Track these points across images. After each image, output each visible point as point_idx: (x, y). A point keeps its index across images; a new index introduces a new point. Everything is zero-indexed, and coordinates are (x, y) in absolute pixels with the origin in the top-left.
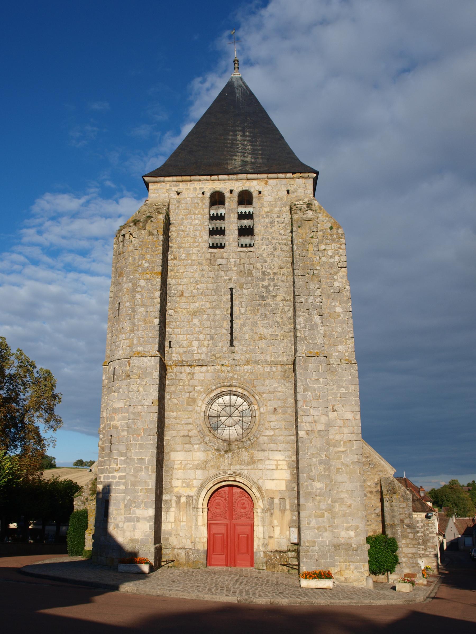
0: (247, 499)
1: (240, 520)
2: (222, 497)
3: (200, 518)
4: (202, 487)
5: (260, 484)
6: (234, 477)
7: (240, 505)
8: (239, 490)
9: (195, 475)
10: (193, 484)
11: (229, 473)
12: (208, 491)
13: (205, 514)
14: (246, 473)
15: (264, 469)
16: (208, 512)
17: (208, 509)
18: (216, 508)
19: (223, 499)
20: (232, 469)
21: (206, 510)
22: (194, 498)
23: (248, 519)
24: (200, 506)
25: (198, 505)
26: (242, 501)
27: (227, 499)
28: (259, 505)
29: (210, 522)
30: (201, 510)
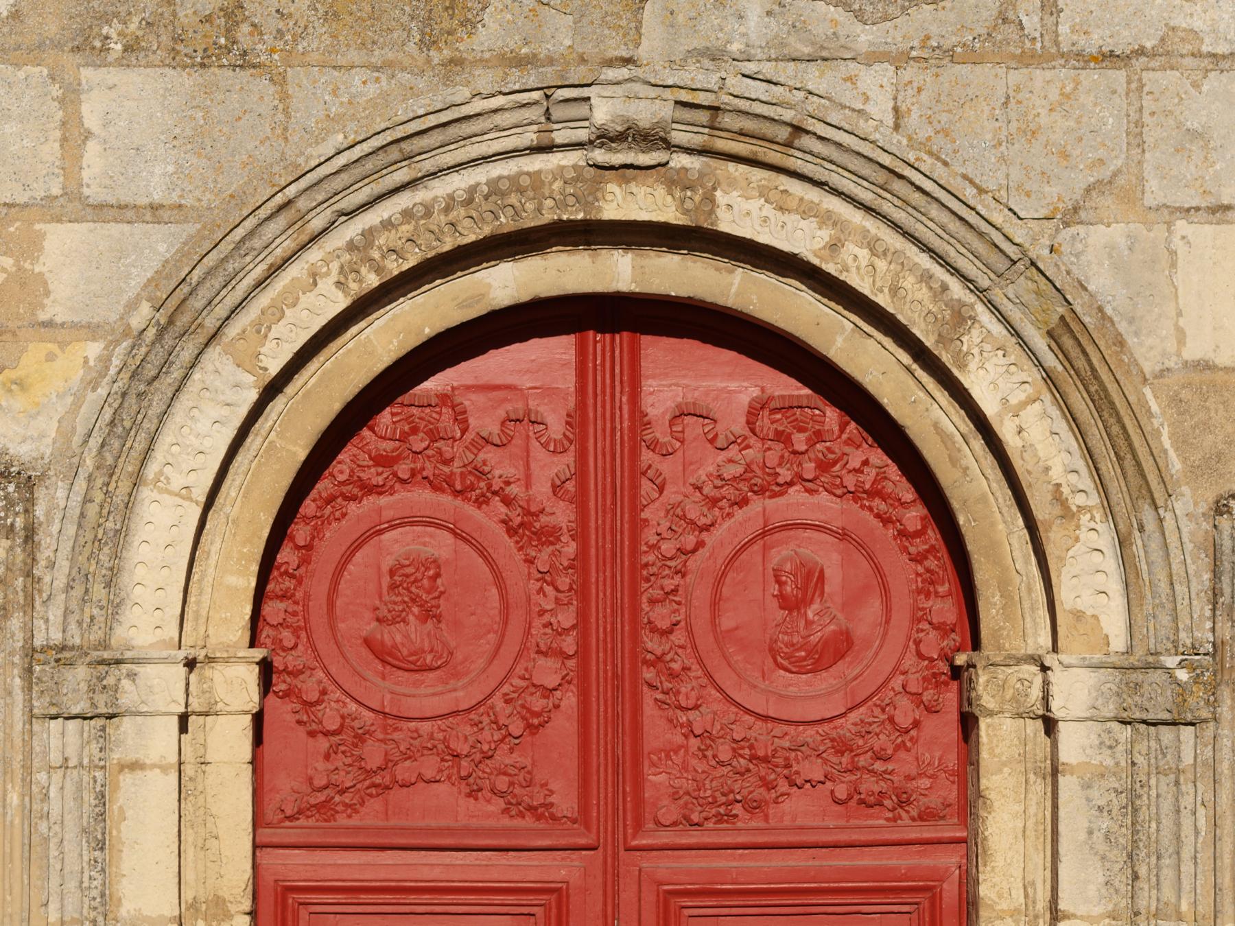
0: (862, 519)
1: (747, 827)
2: (474, 487)
3: (146, 806)
4: (178, 329)
5: (1101, 282)
6: (678, 182)
7: (751, 607)
8: (738, 384)
9: (73, 137)
10: (31, 286)
11: (605, 110)
12: (272, 390)
13: (229, 740)
14: (880, 108)
15: (1162, 53)
16: (258, 720)
17: (266, 670)
18: (381, 653)
19: (487, 521)
20: (651, 46)
21: (237, 685)
22: (57, 502)
23: (876, 824)
24: (146, 620)
25: (114, 608)
26: (783, 553)
27: (561, 515)
28: (1076, 609)
29: (297, 866)
30: (163, 686)
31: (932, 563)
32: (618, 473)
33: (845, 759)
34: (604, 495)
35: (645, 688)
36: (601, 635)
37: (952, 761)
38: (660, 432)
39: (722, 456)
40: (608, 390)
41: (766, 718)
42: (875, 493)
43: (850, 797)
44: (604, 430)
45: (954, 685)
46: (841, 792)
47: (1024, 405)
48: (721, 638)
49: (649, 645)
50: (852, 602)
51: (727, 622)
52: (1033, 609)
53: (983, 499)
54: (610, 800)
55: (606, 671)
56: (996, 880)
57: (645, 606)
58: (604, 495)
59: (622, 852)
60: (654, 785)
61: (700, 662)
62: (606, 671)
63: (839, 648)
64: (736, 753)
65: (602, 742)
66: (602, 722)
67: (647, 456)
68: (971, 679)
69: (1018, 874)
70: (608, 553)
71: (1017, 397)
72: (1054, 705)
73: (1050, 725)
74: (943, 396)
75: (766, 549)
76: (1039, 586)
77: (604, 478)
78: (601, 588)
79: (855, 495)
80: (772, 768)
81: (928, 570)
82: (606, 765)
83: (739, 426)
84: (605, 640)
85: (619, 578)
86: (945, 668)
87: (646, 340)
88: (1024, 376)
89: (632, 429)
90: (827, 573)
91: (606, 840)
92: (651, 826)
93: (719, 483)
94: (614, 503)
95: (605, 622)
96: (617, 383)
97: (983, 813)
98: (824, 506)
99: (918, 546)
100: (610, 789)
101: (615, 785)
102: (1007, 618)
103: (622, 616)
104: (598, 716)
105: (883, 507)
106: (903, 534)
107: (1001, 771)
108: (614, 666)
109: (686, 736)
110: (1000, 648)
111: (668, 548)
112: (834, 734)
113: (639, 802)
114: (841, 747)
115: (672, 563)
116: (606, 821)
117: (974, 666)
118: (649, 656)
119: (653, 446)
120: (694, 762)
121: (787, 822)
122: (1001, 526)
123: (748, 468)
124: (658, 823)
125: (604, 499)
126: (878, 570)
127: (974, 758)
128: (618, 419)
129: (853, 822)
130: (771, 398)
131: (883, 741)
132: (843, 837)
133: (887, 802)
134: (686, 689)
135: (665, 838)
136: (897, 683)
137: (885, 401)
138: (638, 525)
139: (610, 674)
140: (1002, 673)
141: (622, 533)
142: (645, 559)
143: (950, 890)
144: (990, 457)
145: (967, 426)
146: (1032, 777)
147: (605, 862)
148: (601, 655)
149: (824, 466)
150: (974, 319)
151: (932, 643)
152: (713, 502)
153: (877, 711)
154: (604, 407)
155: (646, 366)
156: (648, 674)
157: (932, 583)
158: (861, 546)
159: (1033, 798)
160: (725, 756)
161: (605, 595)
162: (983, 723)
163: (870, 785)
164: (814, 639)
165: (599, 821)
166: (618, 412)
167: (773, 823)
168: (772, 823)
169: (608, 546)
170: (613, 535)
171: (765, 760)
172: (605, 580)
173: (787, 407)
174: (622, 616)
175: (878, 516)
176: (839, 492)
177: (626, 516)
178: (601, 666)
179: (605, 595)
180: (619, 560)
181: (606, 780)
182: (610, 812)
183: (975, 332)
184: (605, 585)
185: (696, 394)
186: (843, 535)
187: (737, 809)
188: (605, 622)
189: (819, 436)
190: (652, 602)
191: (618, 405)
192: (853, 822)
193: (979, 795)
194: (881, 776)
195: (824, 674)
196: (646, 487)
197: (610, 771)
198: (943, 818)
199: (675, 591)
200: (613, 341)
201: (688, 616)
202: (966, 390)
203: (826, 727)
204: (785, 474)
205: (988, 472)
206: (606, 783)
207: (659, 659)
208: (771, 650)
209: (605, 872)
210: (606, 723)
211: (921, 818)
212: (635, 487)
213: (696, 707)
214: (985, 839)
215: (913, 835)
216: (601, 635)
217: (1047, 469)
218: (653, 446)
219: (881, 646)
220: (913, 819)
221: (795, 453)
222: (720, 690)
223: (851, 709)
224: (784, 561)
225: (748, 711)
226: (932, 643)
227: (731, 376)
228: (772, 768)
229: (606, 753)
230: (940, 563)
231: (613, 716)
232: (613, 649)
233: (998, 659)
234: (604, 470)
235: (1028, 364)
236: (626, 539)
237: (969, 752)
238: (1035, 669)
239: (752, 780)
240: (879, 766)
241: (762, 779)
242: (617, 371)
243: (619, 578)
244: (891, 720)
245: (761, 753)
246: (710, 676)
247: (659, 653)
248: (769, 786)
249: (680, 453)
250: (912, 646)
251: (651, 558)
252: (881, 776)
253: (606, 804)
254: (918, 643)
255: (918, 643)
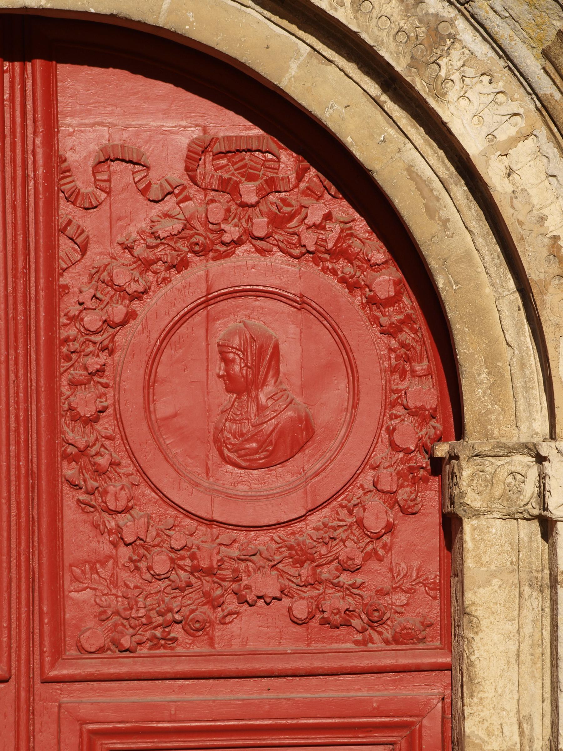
0: (322, 284)
1: (189, 653)
7: (192, 390)
8: (172, 123)
23: (342, 648)
26: (229, 324)
31: (407, 336)
32: (32, 230)
33: (305, 571)
34: (15, 256)
35: (66, 488)
36: (13, 425)
37: (433, 571)
38: (83, 182)
39: (156, 210)
40: (18, 130)
41: (210, 522)
42: (339, 253)
43: (311, 616)
44: (14, 179)
45: (435, 482)
46: (301, 610)
47: (514, 141)
48: (156, 427)
49: (70, 436)
50: (313, 383)
51: (163, 408)
52: (527, 388)
53: (467, 257)
54: (23, 622)
55: (18, 468)
56: (485, 713)
57: (65, 390)
58: (15, 256)
59: (38, 685)
60: (76, 603)
61: (132, 455)
62: (18, 468)
63: (298, 437)
64: (174, 565)
65: (14, 552)
66: (14, 528)
67: (66, 210)
68: (453, 473)
69: (511, 706)
70: (20, 327)
71: (507, 131)
72: (552, 502)
73: (547, 527)
74: (417, 134)
75: (209, 320)
76: (533, 361)
77: (15, 236)
78: (12, 368)
79: (315, 256)
80: (217, 583)
81: (403, 345)
82: (19, 580)
83: (177, 174)
84: (17, 431)
85: (33, 356)
86: (424, 462)
87: (63, 69)
88: (514, 107)
89: (48, 177)
90: (283, 348)
91: (19, 671)
92: (73, 652)
93: (152, 242)
94: (27, 266)
95: (18, 409)
96: (30, 122)
97: (468, 634)
98: (278, 269)
99: (391, 316)
100: (24, 609)
101: (30, 603)
102: (496, 399)
103: (38, 401)
104: (9, 522)
105: (349, 269)
106: (373, 301)
107: (488, 583)
108: (28, 461)
109: (115, 545)
110: (487, 436)
111: (92, 320)
112: (292, 541)
113: (58, 624)
114: (301, 556)
115: (97, 338)
116: (19, 647)
117: (457, 458)
118: (70, 449)
119: (73, 197)
120: (124, 575)
121: (236, 646)
122: (488, 290)
123: (188, 224)
124: (81, 649)
125: (15, 262)
126: (343, 344)
127: (458, 568)
128: (30, 166)
129: (315, 646)
130: (215, 140)
131: (350, 549)
132: (303, 664)
133: (356, 622)
134: (116, 491)
135: (90, 667)
137: (348, 140)
138: (55, 292)
139: (23, 471)
140: (490, 465)
141: (37, 302)
142: (64, 333)
143: (431, 727)
144: (475, 207)
145: (447, 170)
146: (527, 590)
147: (18, 697)
148: (12, 448)
149: (278, 221)
150: (454, 38)
151: (408, 433)
152: (146, 265)
153: (343, 513)
154: (13, 151)
155: (64, 101)
156: (70, 471)
157: (408, 360)
158: (322, 316)
159: (529, 615)
160: (161, 568)
161: (17, 376)
162: (468, 526)
163: (335, 601)
164: (267, 427)
165: (10, 648)
166: (30, 156)
167: (219, 647)
168: (219, 647)
169: (20, 318)
170: (26, 305)
171: (210, 572)
172: (16, 359)
173: (234, 151)
174: (38, 401)
175: (343, 280)
176: (296, 252)
177: (42, 281)
178: (13, 462)
179: (17, 376)
180: (33, 335)
181: (19, 598)
182: (23, 636)
183: (455, 54)
184: (16, 364)
185: (125, 135)
186: (301, 304)
187: (177, 632)
188: (18, 409)
189: (272, 186)
190: (74, 384)
191: (30, 148)
192: (315, 646)
193: (465, 613)
194: (348, 590)
195: (280, 469)
196: (65, 246)
197: (23, 587)
198: (423, 640)
199: (101, 371)
200: (23, 70)
201: (117, 402)
202: (444, 124)
203: (282, 532)
204: (232, 232)
205: (473, 224)
206: (19, 603)
207: (82, 452)
208: (216, 440)
209: (18, 709)
210: (19, 530)
211: (396, 640)
212: (52, 247)
213: (127, 510)
214: (471, 664)
215: (387, 661)
216: (13, 425)
217: (542, 219)
218: (73, 197)
219: (347, 435)
220: (387, 642)
221: (243, 205)
222: (156, 489)
223: (312, 511)
224: (232, 334)
225: (189, 514)
226: (408, 433)
227: (166, 113)
228: (217, 583)
229: (19, 566)
230: (417, 336)
231: (27, 521)
232: (27, 440)
233: (485, 449)
234: (15, 226)
235: (519, 92)
236: (42, 309)
237: (452, 561)
238: (529, 460)
239: (193, 598)
240: (345, 579)
241: (206, 595)
242: (29, 107)
243: (33, 356)
244: (360, 523)
245: (204, 564)
246: (142, 472)
247: (82, 444)
248: (215, 603)
249: (105, 207)
250: (385, 435)
251: (72, 332)
252: (348, 590)
253: (19, 626)
254: (391, 432)
255: (391, 432)
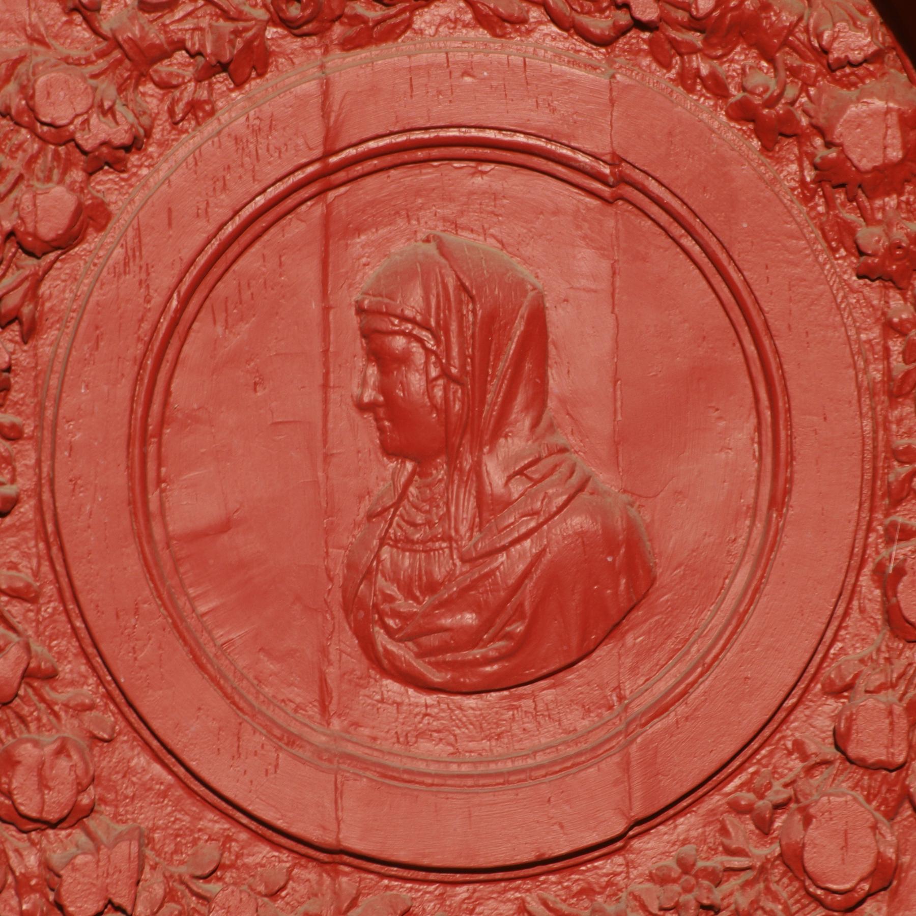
7: (279, 447)
26: (394, 244)
41: (332, 856)
48: (164, 560)
50: (649, 429)
51: (189, 504)
61: (91, 649)
63: (602, 595)
75: (331, 233)
90: (559, 320)
105: (763, 78)
106: (834, 177)
126: (743, 308)
136: (815, 723)
152: (138, 61)
153: (742, 830)
158: (680, 223)
164: (509, 564)
175: (743, 112)
176: (599, 24)
186: (614, 183)
195: (547, 694)
201: (46, 483)
208: (351, 604)
213: (76, 816)
219: (754, 591)
222: (164, 752)
223: (645, 823)
224: (400, 277)
225: (267, 831)
244: (793, 861)
246: (123, 701)
254: (888, 580)
255: (888, 580)
